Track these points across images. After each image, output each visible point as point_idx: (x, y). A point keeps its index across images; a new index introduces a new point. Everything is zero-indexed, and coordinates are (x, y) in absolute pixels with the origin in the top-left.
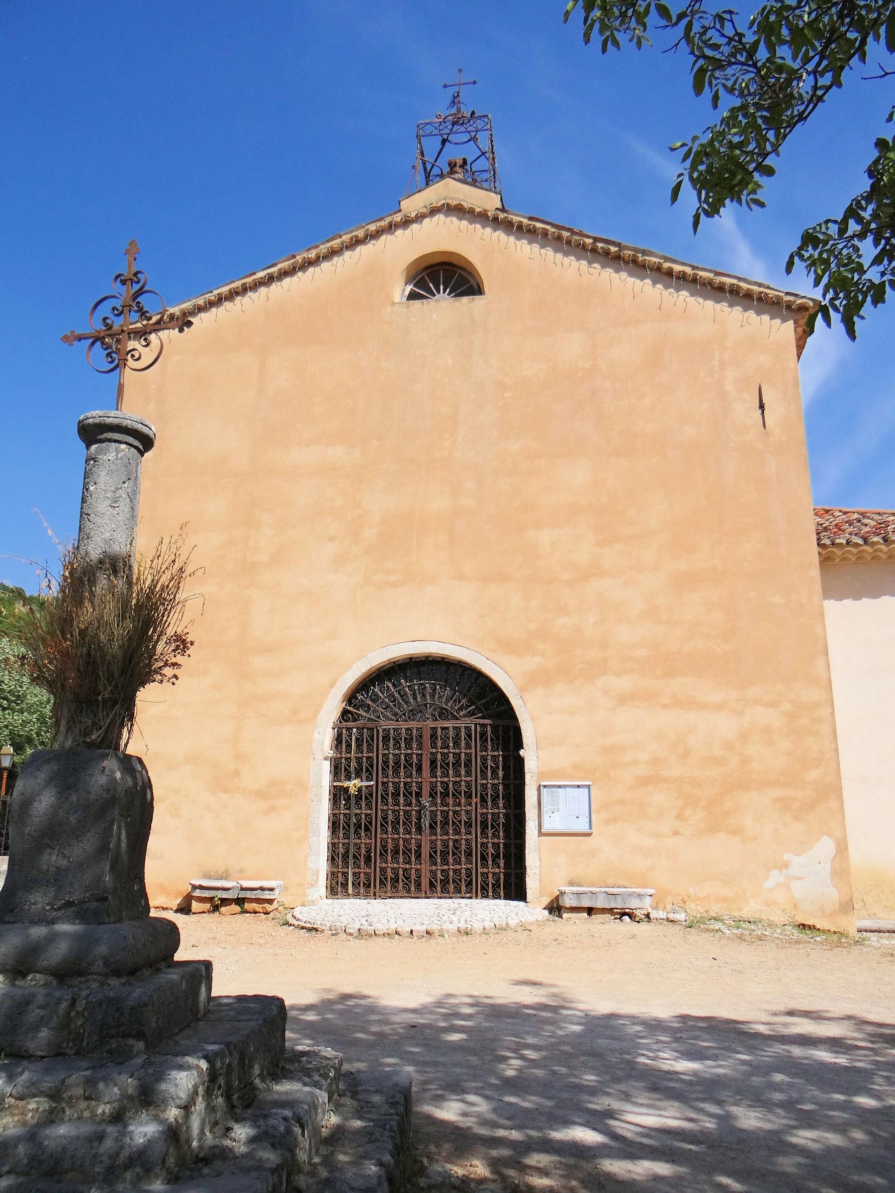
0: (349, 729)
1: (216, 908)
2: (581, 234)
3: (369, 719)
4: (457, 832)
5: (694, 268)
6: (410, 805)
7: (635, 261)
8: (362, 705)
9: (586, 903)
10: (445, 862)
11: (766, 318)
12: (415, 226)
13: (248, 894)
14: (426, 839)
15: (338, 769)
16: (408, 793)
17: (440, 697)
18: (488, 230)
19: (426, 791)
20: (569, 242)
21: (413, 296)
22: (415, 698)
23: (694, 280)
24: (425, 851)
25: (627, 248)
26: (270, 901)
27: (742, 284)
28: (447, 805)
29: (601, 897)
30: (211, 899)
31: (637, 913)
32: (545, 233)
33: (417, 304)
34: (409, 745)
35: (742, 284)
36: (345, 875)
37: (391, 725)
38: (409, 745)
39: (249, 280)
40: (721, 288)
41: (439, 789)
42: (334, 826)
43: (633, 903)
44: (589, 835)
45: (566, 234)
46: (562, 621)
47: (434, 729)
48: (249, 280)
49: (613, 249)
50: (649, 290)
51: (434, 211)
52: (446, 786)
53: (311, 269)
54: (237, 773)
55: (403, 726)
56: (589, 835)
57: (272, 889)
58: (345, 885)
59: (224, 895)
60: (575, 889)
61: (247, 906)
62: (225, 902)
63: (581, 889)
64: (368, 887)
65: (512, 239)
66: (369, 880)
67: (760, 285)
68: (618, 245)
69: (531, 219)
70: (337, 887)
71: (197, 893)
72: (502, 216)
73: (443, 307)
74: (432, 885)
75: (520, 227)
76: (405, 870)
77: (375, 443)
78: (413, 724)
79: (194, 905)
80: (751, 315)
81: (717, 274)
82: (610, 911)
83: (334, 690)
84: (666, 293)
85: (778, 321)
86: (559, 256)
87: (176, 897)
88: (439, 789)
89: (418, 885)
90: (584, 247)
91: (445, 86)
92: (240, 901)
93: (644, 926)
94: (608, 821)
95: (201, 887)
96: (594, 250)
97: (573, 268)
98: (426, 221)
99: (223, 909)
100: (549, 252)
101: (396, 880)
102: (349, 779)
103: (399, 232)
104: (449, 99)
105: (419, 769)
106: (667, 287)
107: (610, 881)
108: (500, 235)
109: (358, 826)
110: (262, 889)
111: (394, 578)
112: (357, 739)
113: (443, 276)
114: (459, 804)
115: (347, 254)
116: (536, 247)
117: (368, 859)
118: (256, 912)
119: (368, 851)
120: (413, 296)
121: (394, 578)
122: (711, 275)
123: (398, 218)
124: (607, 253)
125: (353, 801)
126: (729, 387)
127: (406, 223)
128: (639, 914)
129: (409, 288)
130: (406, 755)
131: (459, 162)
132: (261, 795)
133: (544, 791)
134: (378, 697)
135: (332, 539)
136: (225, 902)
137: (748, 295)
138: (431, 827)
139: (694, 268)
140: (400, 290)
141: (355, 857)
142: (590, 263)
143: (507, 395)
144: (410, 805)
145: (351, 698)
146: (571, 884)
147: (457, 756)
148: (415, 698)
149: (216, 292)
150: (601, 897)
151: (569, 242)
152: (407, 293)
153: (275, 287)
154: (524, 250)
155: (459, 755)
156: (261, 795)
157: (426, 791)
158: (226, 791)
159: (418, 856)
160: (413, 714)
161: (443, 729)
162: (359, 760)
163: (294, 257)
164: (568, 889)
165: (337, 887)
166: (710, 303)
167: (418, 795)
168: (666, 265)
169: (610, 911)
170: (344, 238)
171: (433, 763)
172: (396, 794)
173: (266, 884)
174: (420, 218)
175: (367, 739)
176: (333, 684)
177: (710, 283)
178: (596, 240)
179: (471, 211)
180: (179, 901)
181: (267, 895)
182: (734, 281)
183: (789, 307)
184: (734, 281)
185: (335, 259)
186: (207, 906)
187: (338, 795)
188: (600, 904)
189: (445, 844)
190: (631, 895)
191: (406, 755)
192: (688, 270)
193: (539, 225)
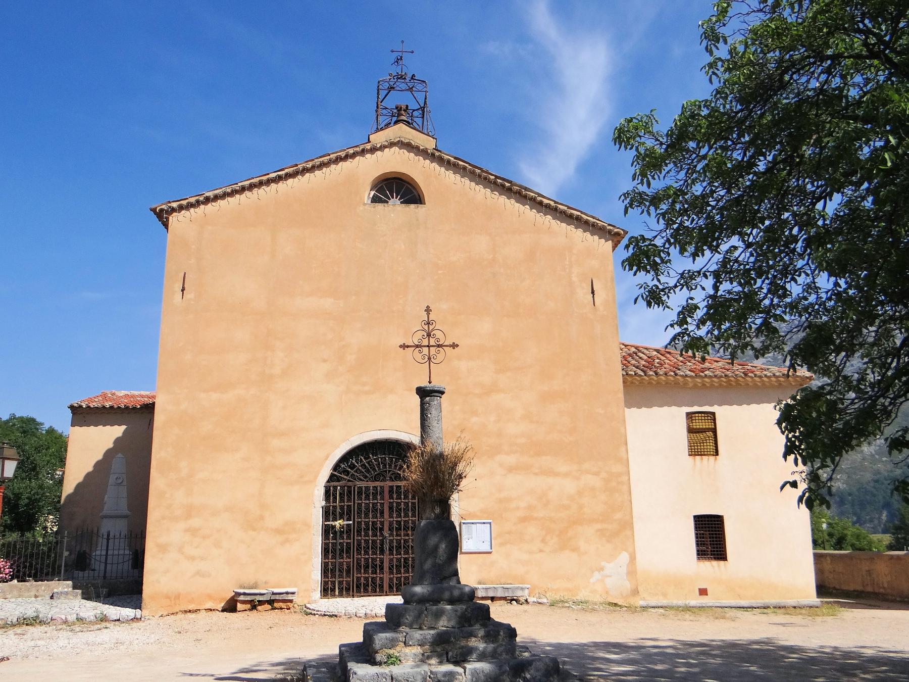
0: (335, 487)
1: (254, 607)
2: (487, 172)
3: (349, 481)
4: (407, 553)
5: (555, 202)
6: (376, 536)
7: (519, 193)
8: (346, 472)
9: (491, 594)
10: (399, 572)
11: (596, 237)
12: (379, 153)
13: (277, 597)
14: (386, 558)
15: (328, 513)
16: (374, 529)
17: (396, 466)
18: (428, 161)
19: (386, 527)
20: (480, 176)
21: (375, 200)
22: (379, 467)
23: (556, 209)
24: (386, 565)
25: (516, 185)
26: (291, 601)
27: (583, 216)
28: (400, 536)
29: (500, 590)
30: (251, 602)
31: (520, 599)
32: (465, 168)
33: (380, 206)
34: (375, 498)
35: (583, 216)
36: (333, 583)
37: (363, 484)
38: (375, 498)
39: (265, 178)
40: (571, 216)
41: (395, 525)
42: (326, 551)
43: (519, 593)
44: (490, 553)
45: (478, 171)
46: (474, 419)
47: (391, 487)
48: (265, 178)
49: (507, 184)
50: (527, 212)
51: (392, 144)
52: (399, 523)
53: (308, 175)
54: (262, 518)
55: (371, 484)
56: (490, 553)
57: (293, 593)
58: (333, 590)
59: (261, 599)
60: (484, 586)
61: (276, 605)
62: (261, 603)
63: (488, 586)
64: (348, 590)
65: (443, 169)
66: (349, 586)
67: (593, 218)
68: (510, 182)
69: (455, 158)
70: (327, 591)
71: (242, 598)
72: (437, 154)
73: (395, 208)
74: (391, 587)
75: (449, 162)
76: (372, 578)
77: (354, 297)
78: (377, 484)
79: (240, 606)
80: (588, 234)
81: (569, 208)
82: (505, 598)
83: (328, 462)
84: (538, 215)
85: (603, 240)
86: (473, 184)
87: (221, 602)
88: (395, 525)
89: (381, 587)
90: (490, 181)
91: (393, 51)
92: (271, 602)
93: (525, 607)
94: (502, 545)
95: (245, 594)
96: (495, 183)
97: (481, 193)
98: (387, 150)
99: (259, 608)
100: (466, 181)
101: (358, 587)
102: (335, 520)
103: (368, 156)
104: (393, 59)
105: (382, 513)
106: (538, 212)
107: (503, 581)
108: (435, 165)
109: (342, 551)
110: (287, 593)
111: (367, 388)
112: (340, 494)
113: (397, 188)
114: (408, 535)
115: (333, 166)
116: (458, 177)
117: (348, 571)
118: (281, 609)
119: (349, 567)
120: (375, 200)
121: (367, 388)
122: (566, 208)
123: (368, 146)
124: (503, 186)
125: (338, 534)
126: (574, 279)
127: (373, 150)
128: (522, 599)
129: (373, 193)
130: (373, 504)
131: (404, 107)
132: (278, 531)
133: (463, 526)
134: (355, 466)
135: (325, 361)
136: (261, 603)
137: (587, 222)
138: (390, 550)
139: (555, 202)
140: (368, 194)
141: (340, 571)
142: (492, 191)
143: (440, 272)
144: (376, 536)
145: (336, 467)
146: (480, 583)
147: (406, 504)
148: (379, 467)
149: (240, 184)
150: (500, 590)
151: (480, 176)
152: (371, 196)
153: (281, 185)
154: (451, 178)
155: (408, 503)
156: (278, 531)
157: (386, 527)
158: (254, 530)
159: (382, 568)
160: (375, 479)
161: (397, 487)
162: (342, 508)
163: (297, 165)
164: (480, 586)
165: (327, 591)
166: (564, 225)
167: (382, 529)
168: (539, 199)
169: (505, 598)
170: (332, 156)
171: (391, 508)
172: (367, 529)
173: (290, 590)
174: (382, 148)
175: (348, 493)
176: (327, 458)
177: (564, 212)
178: (497, 177)
179: (417, 148)
180: (222, 605)
181: (290, 597)
182: (579, 213)
183: (610, 232)
184: (579, 213)
185: (324, 169)
186: (249, 606)
187: (327, 531)
188: (499, 595)
189: (399, 560)
190: (517, 588)
191: (373, 504)
192: (552, 203)
193: (461, 163)
